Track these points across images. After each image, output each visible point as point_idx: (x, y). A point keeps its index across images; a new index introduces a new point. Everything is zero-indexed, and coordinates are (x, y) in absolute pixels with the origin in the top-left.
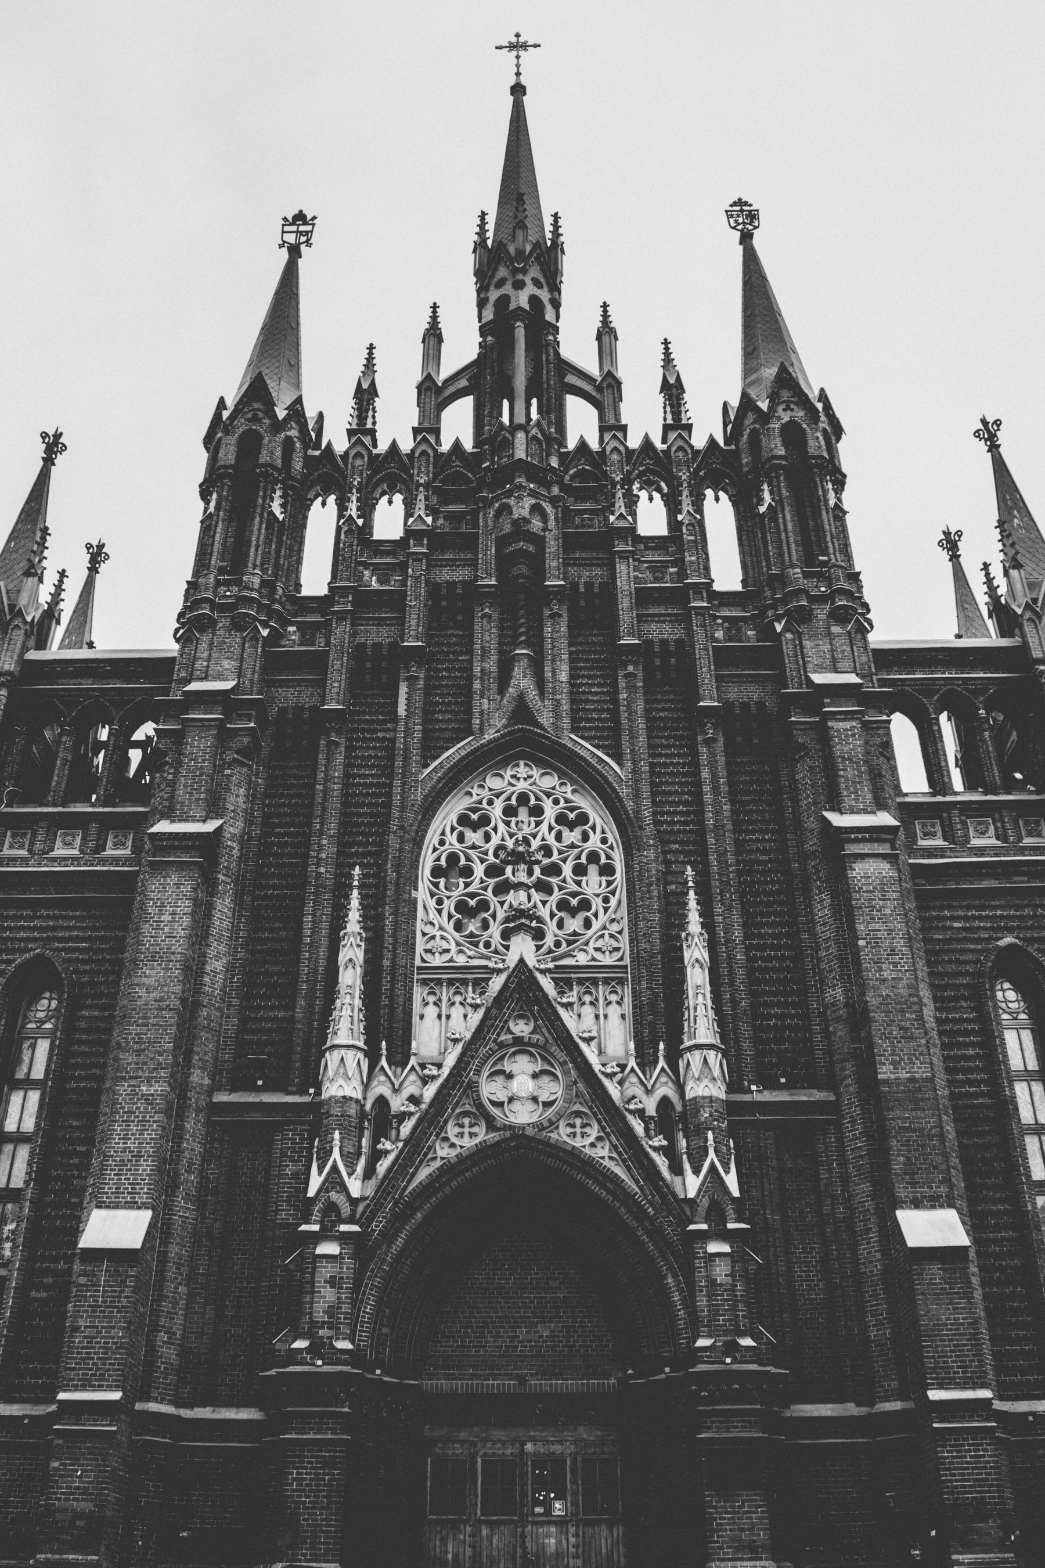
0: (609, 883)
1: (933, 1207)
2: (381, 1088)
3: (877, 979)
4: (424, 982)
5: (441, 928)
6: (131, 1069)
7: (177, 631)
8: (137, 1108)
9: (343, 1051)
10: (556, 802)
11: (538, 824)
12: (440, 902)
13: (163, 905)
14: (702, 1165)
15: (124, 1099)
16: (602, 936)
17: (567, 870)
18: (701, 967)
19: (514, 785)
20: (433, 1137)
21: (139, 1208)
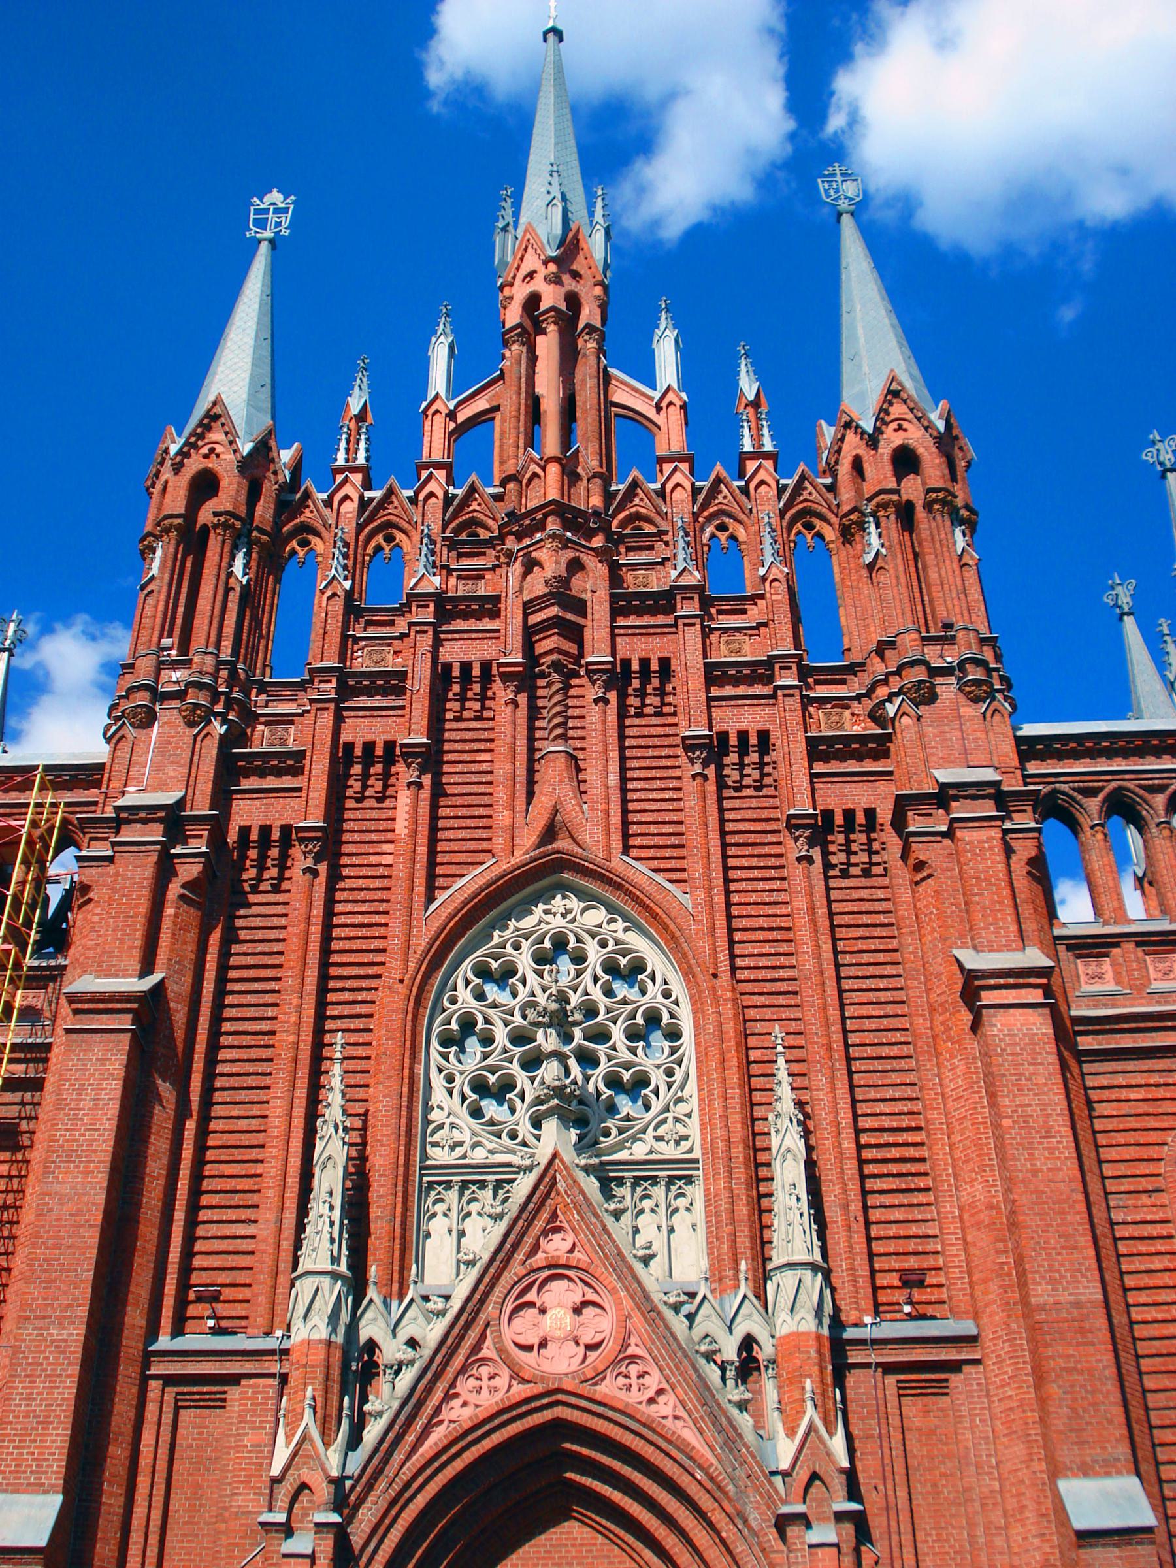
0: (673, 1051)
1: (1108, 1474)
3: (1027, 1171)
6: (38, 1306)
7: (108, 728)
8: (47, 1358)
9: (316, 1280)
10: (603, 944)
11: (579, 974)
12: (450, 1079)
13: (82, 1088)
14: (798, 1425)
15: (27, 1347)
16: (664, 1121)
17: (617, 1033)
19: (548, 923)
21: (46, 1492)
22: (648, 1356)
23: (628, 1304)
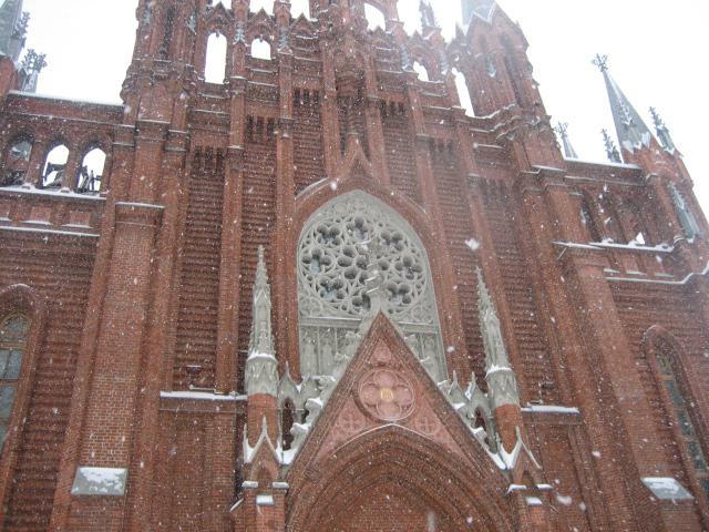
5: (312, 295)
10: (381, 225)
12: (310, 279)
17: (392, 266)
18: (495, 325)
23: (421, 387)
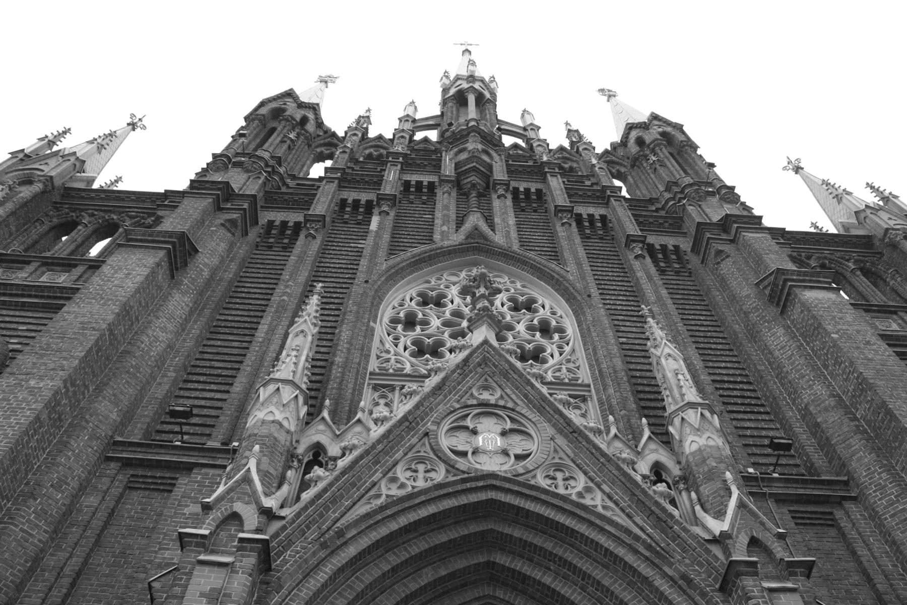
2: (319, 434)
4: (376, 388)
12: (397, 338)
20: (379, 475)
22: (572, 464)
